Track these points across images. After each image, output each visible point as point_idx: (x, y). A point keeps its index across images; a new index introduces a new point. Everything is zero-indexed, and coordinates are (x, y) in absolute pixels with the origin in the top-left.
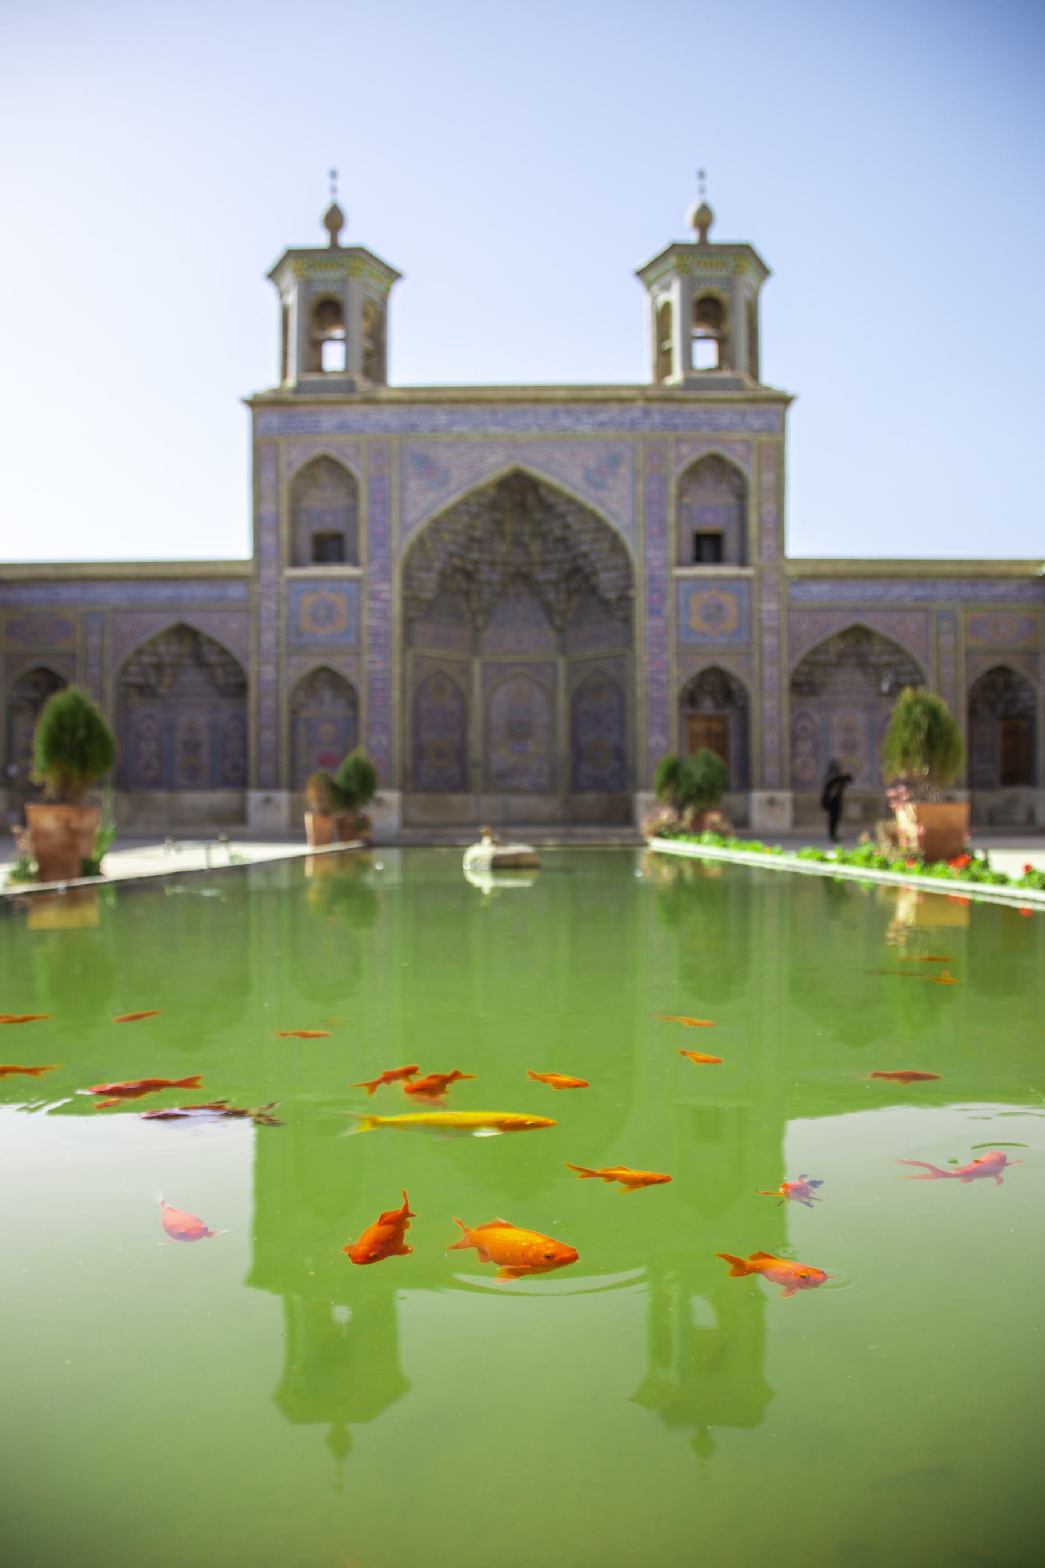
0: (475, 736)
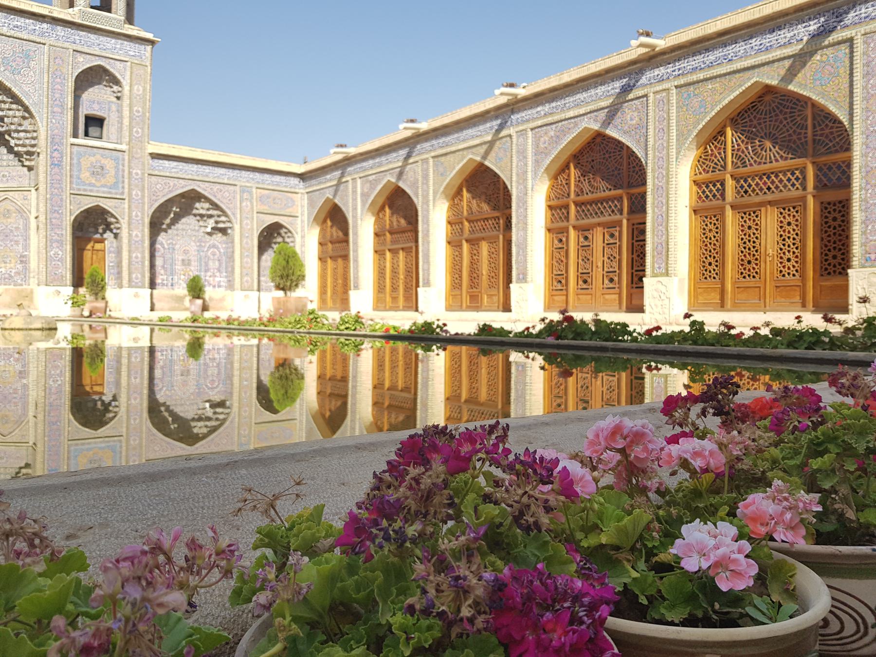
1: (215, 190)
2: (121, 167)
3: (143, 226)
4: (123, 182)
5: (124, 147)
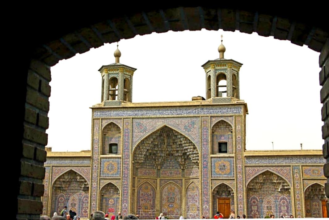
0: (157, 202)
1: (279, 170)
2: (232, 164)
3: (243, 191)
4: (234, 171)
5: (233, 155)
